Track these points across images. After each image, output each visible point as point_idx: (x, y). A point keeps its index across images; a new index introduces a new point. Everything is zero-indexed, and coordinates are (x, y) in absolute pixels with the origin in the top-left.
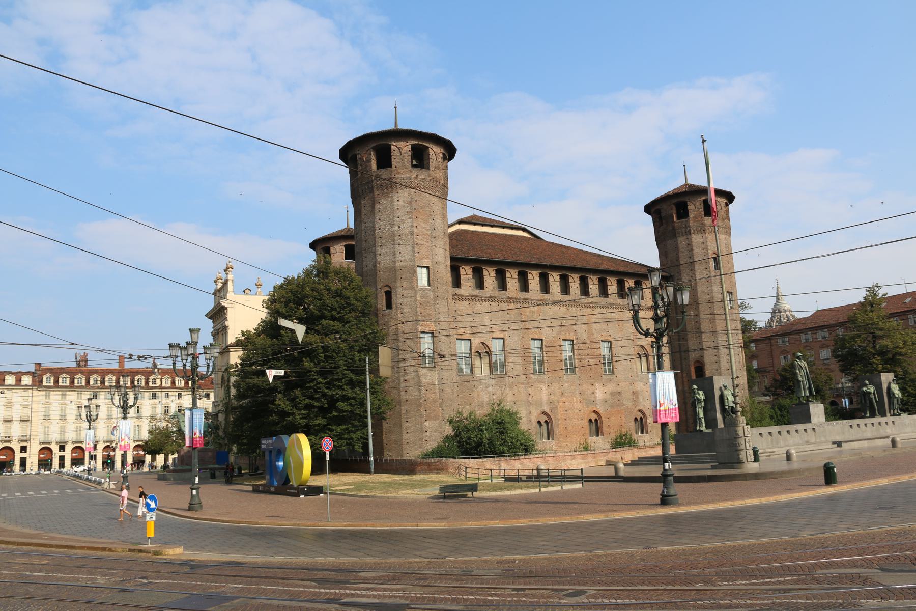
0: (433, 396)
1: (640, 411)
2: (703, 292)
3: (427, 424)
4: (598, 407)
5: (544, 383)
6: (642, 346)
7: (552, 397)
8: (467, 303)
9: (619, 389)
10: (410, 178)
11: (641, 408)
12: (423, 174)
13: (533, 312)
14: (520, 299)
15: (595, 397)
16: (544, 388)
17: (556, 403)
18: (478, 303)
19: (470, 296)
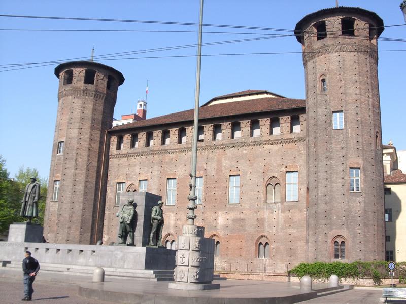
0: (54, 218)
1: (263, 236)
2: (311, 117)
3: (49, 235)
4: (219, 231)
5: (173, 212)
6: (273, 177)
7: (178, 222)
8: (126, 158)
9: (242, 216)
10: (62, 92)
11: (266, 234)
12: (69, 87)
13: (172, 159)
14: (162, 150)
15: (217, 223)
16: (172, 215)
17: (181, 227)
18: (133, 158)
19: (128, 153)
